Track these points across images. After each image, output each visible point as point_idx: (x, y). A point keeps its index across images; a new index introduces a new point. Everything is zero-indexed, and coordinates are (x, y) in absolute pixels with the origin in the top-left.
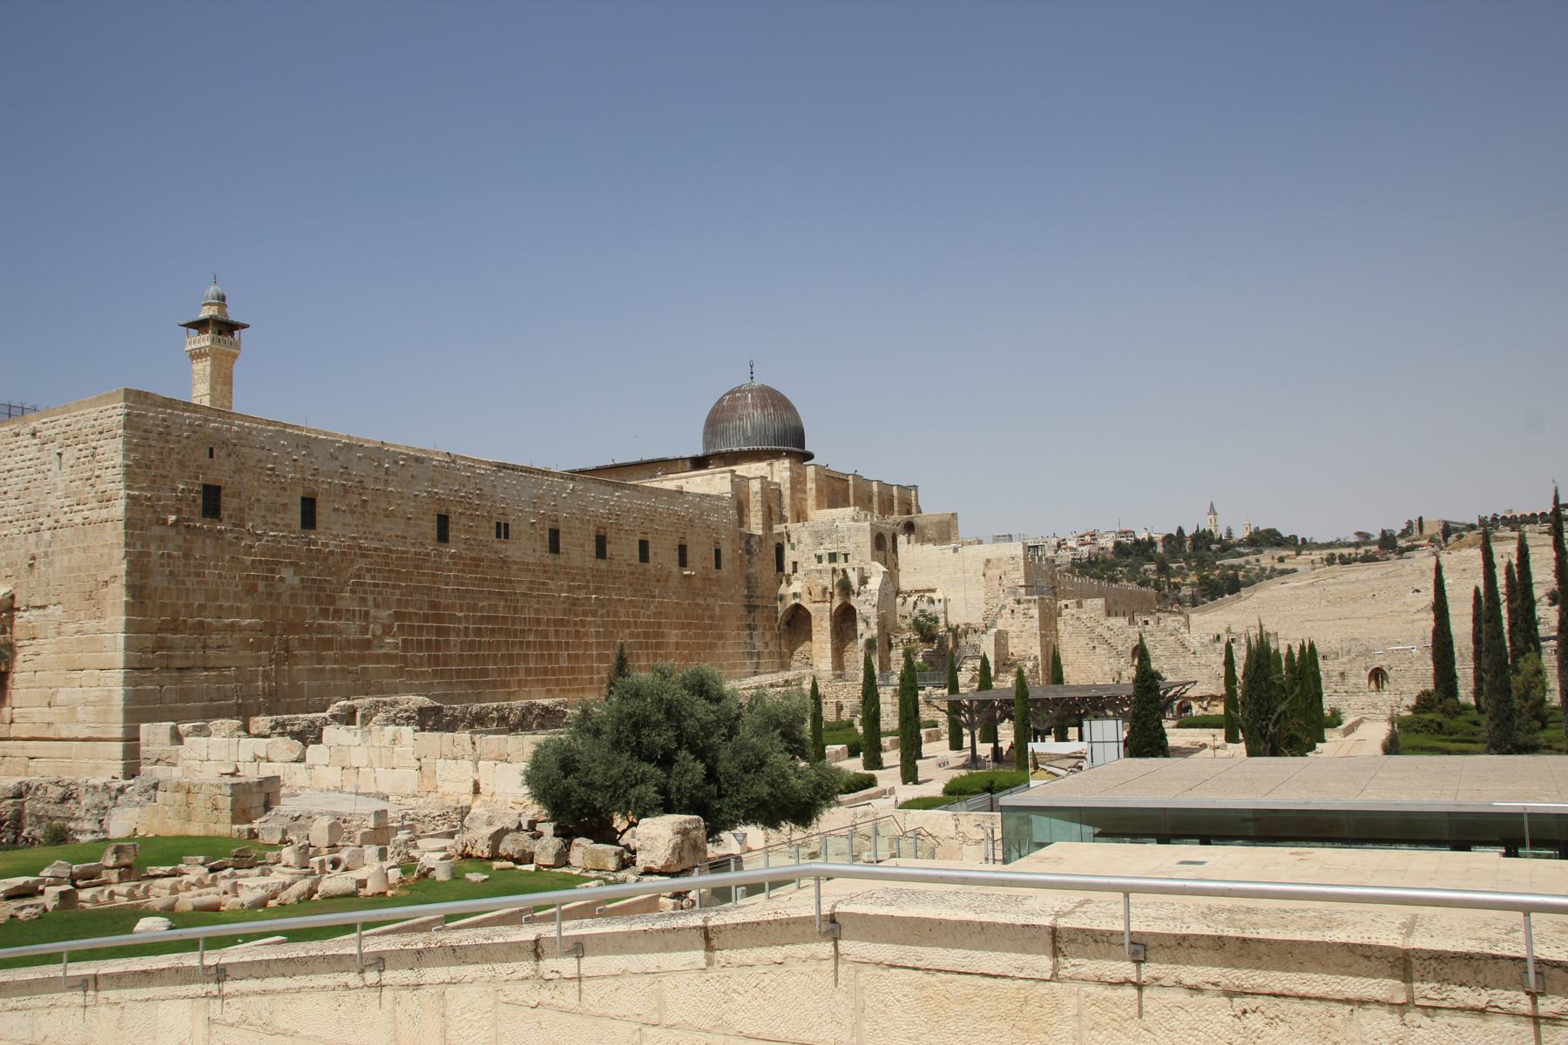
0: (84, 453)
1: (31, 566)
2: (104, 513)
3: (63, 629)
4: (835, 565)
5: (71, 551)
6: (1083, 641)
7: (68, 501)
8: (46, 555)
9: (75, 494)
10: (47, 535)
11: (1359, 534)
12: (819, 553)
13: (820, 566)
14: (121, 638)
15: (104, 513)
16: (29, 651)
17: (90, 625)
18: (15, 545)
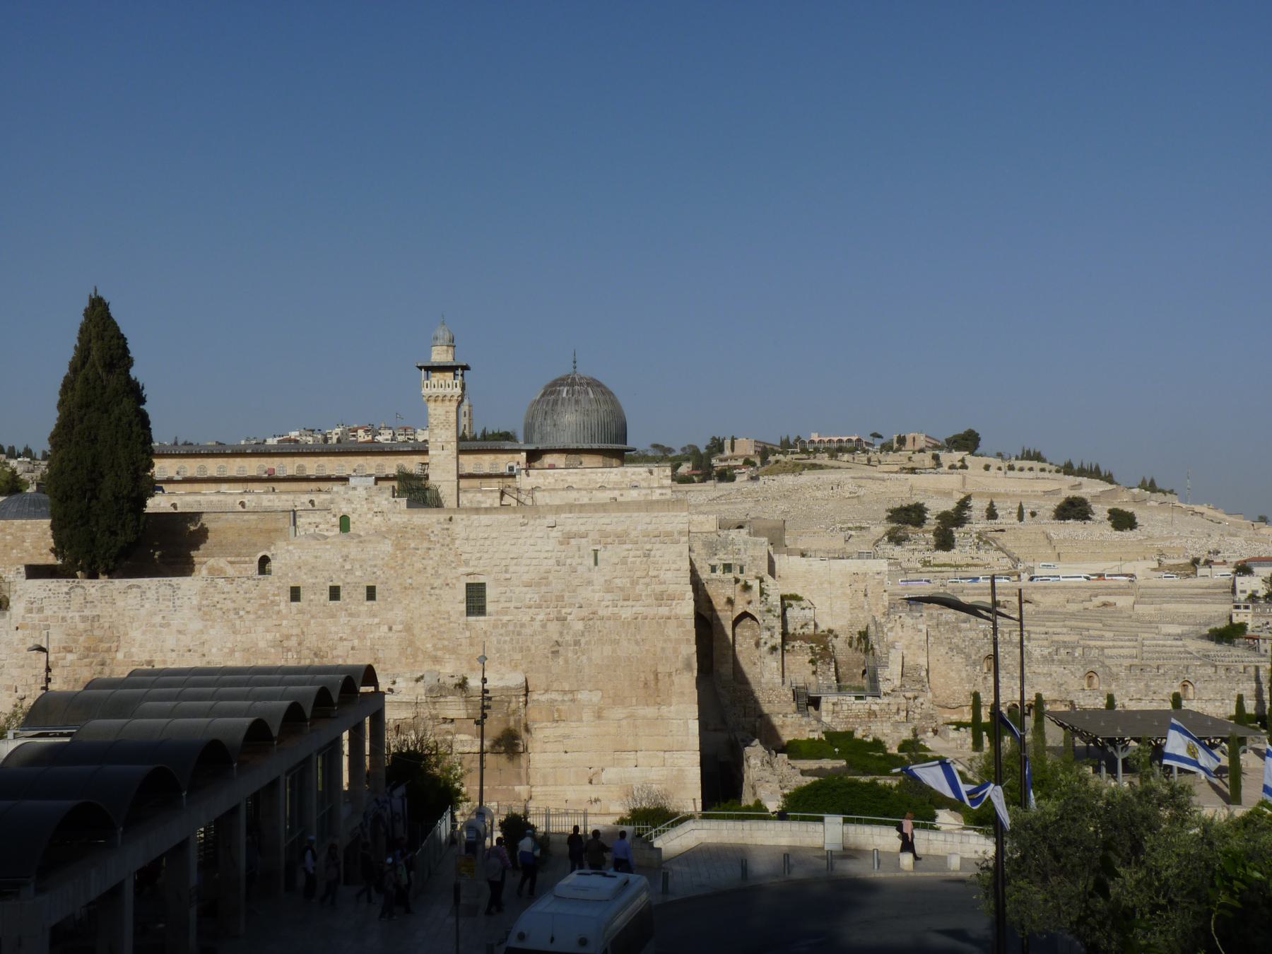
0: (631, 553)
1: (553, 652)
2: (664, 611)
3: (605, 713)
4: (730, 576)
5: (617, 642)
6: (943, 650)
7: (609, 596)
8: (577, 643)
9: (622, 589)
10: (579, 626)
11: (656, 446)
12: (713, 563)
13: (713, 575)
14: (694, 726)
15: (664, 611)
16: (547, 732)
17: (650, 711)
18: (528, 631)
